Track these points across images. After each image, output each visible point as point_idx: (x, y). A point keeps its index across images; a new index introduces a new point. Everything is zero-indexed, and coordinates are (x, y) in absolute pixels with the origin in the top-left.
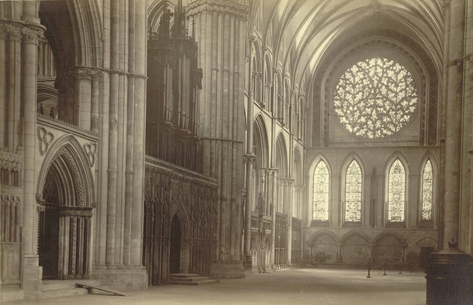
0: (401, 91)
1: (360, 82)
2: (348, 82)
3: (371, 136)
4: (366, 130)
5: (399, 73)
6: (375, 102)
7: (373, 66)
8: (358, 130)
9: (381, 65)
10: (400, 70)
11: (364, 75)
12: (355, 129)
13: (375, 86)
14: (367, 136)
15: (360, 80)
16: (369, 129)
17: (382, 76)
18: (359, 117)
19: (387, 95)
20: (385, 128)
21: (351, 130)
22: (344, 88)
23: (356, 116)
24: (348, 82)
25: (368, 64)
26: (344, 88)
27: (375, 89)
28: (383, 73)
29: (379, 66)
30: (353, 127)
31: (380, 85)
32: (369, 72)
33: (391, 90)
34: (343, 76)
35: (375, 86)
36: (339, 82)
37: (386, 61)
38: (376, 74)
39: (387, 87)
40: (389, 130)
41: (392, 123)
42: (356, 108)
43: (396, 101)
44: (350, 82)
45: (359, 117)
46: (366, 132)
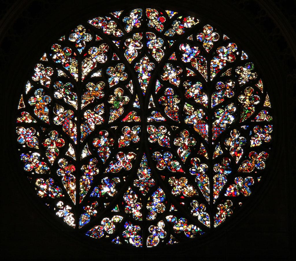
0: (226, 102)
1: (97, 75)
2: (61, 73)
3: (133, 241)
4: (117, 219)
5: (213, 53)
6: (144, 135)
7: (135, 30)
8: (95, 221)
9: (160, 27)
10: (217, 45)
11: (108, 54)
12: (85, 218)
13: (144, 88)
14: (122, 239)
15: (94, 70)
16: (129, 218)
17: (165, 60)
18: (97, 182)
19: (183, 114)
20: (178, 215)
21: (70, 220)
22: (49, 91)
23: (86, 179)
24: (61, 73)
25: (121, 25)
26: (49, 91)
27: (144, 101)
28: (168, 53)
29: (153, 30)
30: (77, 212)
31: (158, 83)
32: (123, 49)
33: (191, 101)
34: (45, 55)
35: (144, 88)
36: (33, 73)
37: (175, 18)
38: (145, 52)
39: (180, 92)
40: (193, 220)
41: (201, 199)
42: (84, 154)
43: (211, 133)
44: (67, 72)
45: (97, 182)
46: (120, 227)
